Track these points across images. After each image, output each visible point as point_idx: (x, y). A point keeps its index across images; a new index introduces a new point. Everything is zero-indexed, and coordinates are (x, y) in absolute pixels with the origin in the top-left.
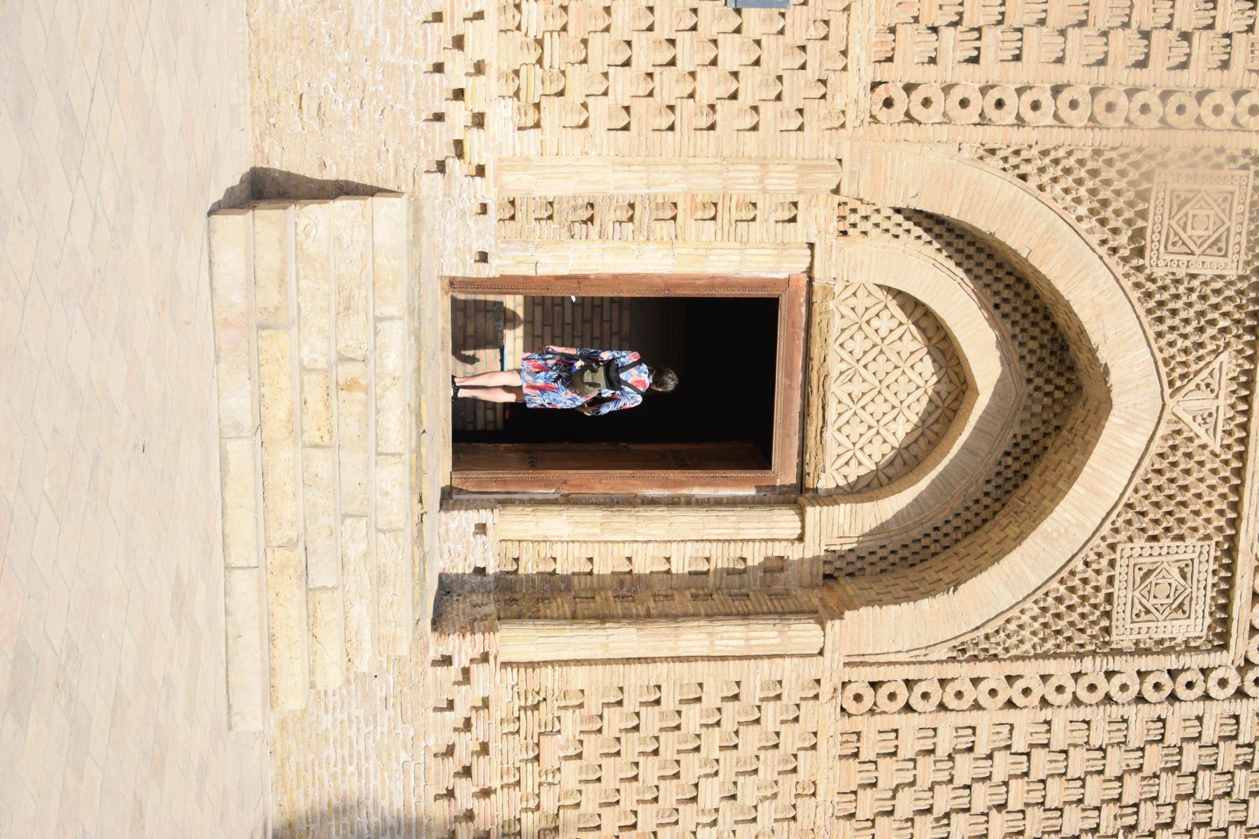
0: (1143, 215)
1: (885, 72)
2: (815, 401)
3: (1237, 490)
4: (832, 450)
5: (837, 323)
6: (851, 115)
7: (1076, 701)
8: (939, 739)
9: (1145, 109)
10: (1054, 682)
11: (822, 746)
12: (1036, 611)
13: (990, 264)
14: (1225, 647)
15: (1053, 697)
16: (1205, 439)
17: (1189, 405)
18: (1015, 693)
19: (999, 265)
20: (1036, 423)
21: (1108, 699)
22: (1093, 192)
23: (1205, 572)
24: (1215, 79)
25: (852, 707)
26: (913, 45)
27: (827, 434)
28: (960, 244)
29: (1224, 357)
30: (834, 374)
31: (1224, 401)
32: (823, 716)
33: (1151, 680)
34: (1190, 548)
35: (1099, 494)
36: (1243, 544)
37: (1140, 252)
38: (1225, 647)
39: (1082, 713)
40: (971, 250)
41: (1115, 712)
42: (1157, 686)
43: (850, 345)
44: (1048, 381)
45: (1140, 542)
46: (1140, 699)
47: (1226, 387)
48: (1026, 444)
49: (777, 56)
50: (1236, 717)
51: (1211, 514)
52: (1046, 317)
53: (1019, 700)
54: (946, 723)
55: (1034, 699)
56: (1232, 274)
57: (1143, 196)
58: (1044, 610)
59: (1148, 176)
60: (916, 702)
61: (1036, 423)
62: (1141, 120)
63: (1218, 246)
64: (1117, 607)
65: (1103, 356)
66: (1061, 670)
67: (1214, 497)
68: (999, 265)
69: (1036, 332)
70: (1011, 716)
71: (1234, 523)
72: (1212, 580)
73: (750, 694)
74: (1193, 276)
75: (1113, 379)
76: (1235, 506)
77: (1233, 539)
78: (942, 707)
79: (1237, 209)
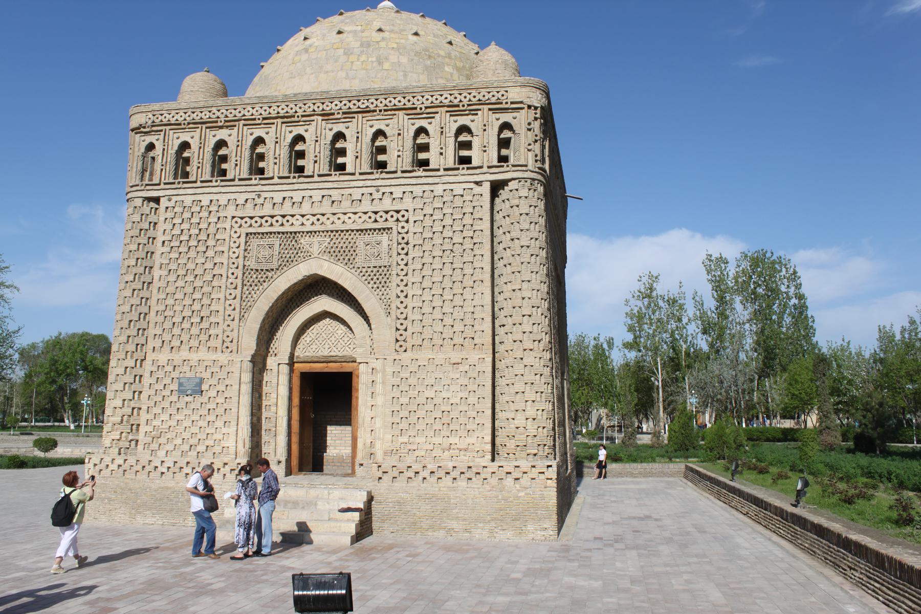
0: (262, 270)
1: (219, 349)
2: (332, 359)
3: (342, 231)
4: (345, 353)
5: (307, 354)
6: (230, 358)
7: (406, 275)
8: (416, 319)
9: (233, 274)
10: (399, 283)
11: (416, 357)
12: (378, 290)
13: (286, 310)
14: (391, 228)
15: (404, 283)
16: (326, 244)
17: (315, 250)
18: (402, 295)
19: (286, 307)
20: (333, 291)
21: (406, 265)
22: (256, 285)
23: (367, 238)
24: (226, 254)
25: (403, 348)
26: (212, 343)
27: (341, 355)
28: (280, 319)
29: (302, 241)
30: (322, 354)
31: (315, 239)
32: (406, 357)
33: (400, 251)
34: (360, 244)
35: (342, 274)
36: (358, 228)
37: (272, 270)
38: (391, 228)
39: (410, 272)
40: (282, 316)
41: (410, 262)
42: (403, 249)
43: (314, 349)
44: (321, 289)
45: (357, 260)
46: (407, 254)
47: (312, 239)
48: (340, 294)
49: (214, 381)
50: (415, 222)
51: (350, 238)
52: (302, 291)
53: (405, 294)
54: (410, 317)
55: (404, 289)
56: (278, 243)
57: (257, 270)
58: (378, 288)
59: (252, 270)
60: (403, 327)
61: (333, 291)
62: (235, 275)
63: (271, 247)
64: (377, 265)
65: (300, 278)
66: (395, 280)
67: (350, 238)
68: (286, 307)
69: (306, 294)
70: (410, 296)
71: (353, 231)
72: (371, 236)
73: (397, 381)
74: (279, 253)
75: (308, 274)
76: (347, 231)
77: (357, 231)
78: (406, 319)
79: (262, 243)
